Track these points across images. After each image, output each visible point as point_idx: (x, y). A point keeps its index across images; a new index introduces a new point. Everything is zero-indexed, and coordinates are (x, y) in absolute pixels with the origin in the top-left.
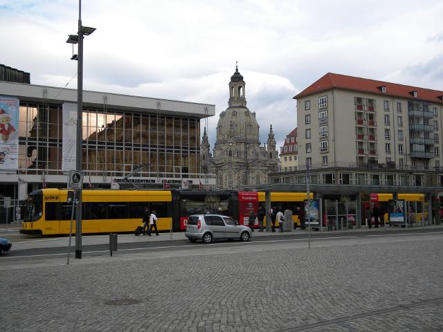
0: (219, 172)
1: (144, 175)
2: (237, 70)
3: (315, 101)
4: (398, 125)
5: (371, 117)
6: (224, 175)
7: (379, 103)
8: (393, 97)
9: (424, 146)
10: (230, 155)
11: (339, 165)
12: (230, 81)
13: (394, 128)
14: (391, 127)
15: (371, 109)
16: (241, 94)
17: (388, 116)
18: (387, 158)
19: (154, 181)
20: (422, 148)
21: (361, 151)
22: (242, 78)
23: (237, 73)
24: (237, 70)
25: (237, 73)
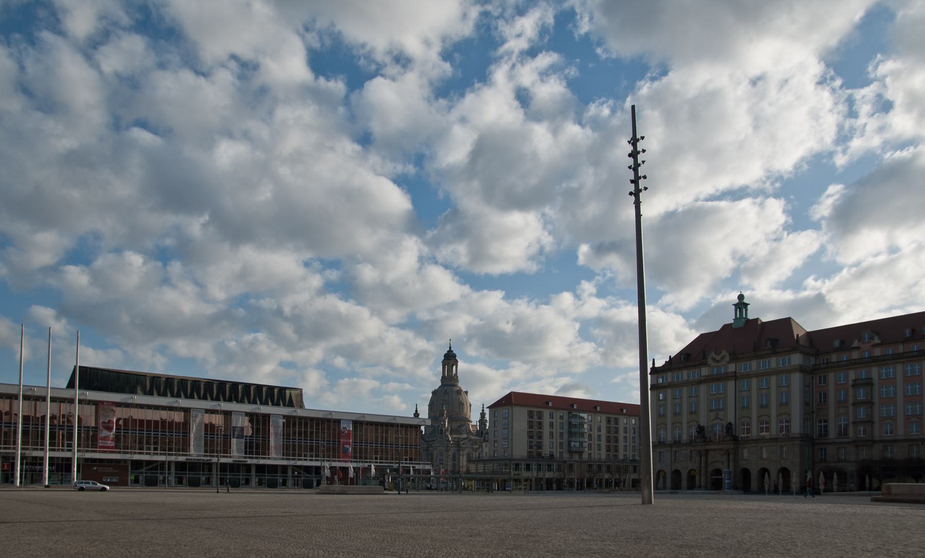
0: (430, 449)
1: (386, 463)
2: (450, 348)
3: (504, 411)
4: (560, 428)
5: (540, 423)
6: (435, 452)
7: (546, 413)
8: (557, 409)
9: (578, 443)
10: (442, 433)
11: (514, 457)
12: (443, 359)
13: (557, 430)
14: (554, 430)
15: (540, 418)
16: (454, 372)
17: (550, 420)
18: (550, 452)
19: (392, 466)
20: (577, 444)
21: (531, 447)
22: (455, 356)
23: (450, 351)
24: (450, 348)
25: (450, 351)
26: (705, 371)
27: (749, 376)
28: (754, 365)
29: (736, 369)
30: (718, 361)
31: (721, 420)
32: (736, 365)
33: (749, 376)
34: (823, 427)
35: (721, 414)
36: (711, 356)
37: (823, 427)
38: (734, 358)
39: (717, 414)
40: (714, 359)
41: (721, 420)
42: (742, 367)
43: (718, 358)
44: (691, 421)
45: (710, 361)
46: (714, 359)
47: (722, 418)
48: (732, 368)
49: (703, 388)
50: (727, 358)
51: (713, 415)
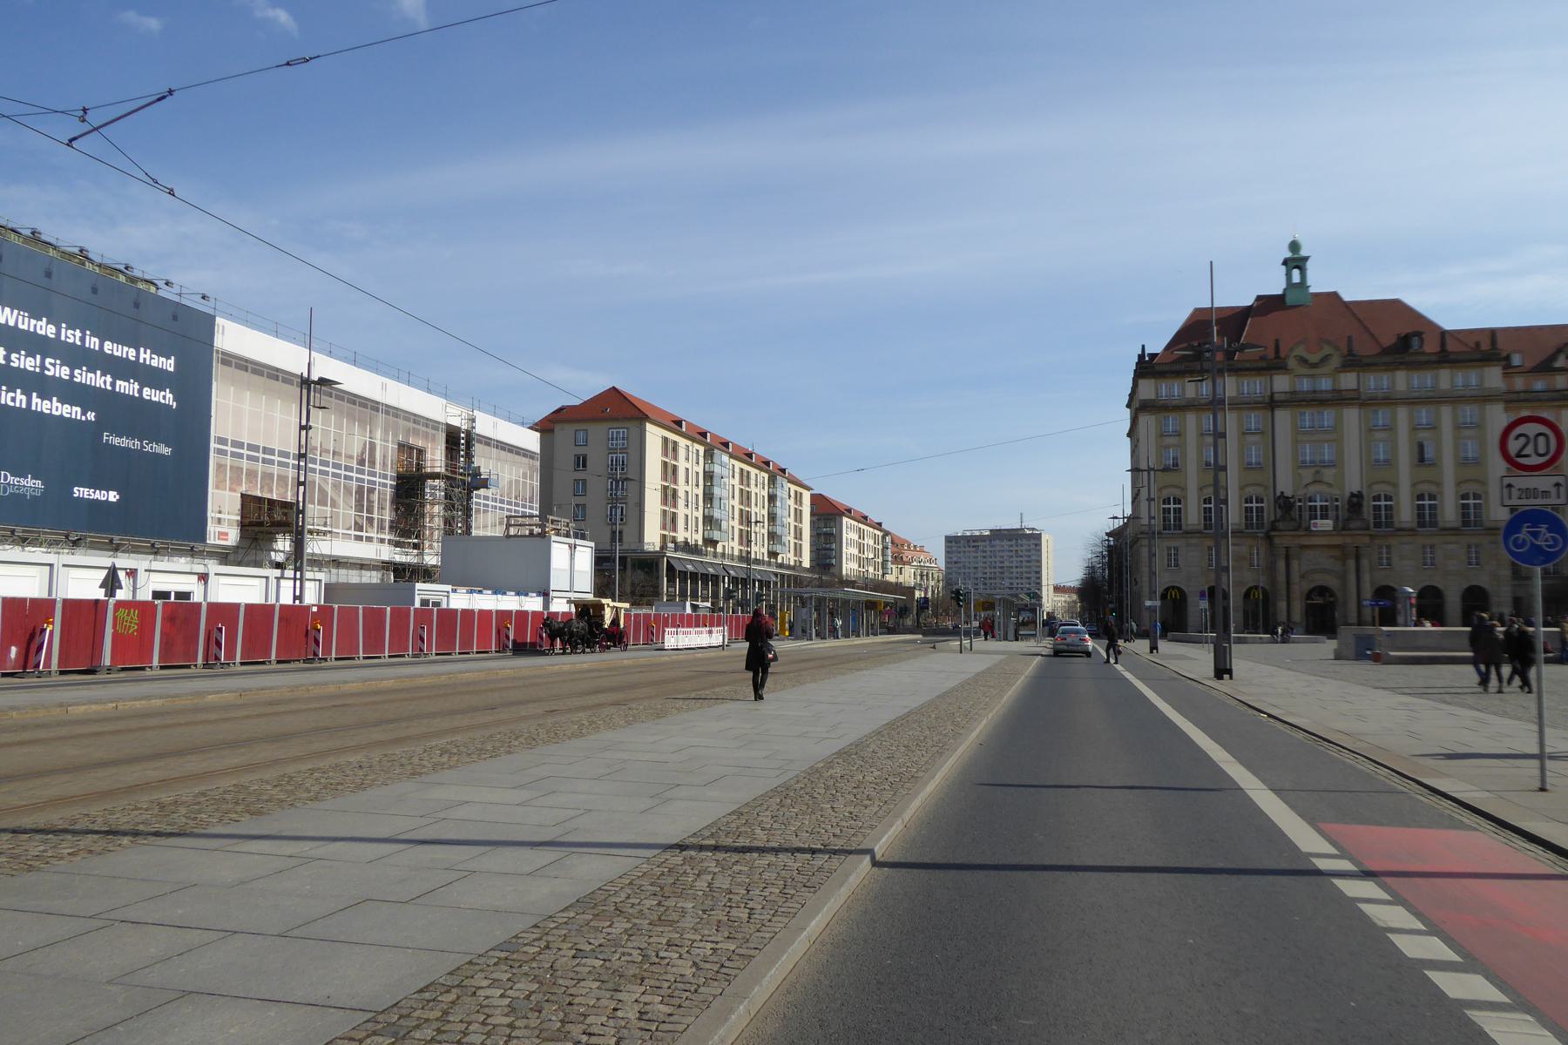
26: (1281, 383)
27: (1389, 401)
28: (1402, 381)
29: (1359, 384)
30: (1314, 366)
31: (1330, 485)
32: (1358, 375)
33: (1389, 401)
34: (1319, 510)
35: (1328, 474)
36: (1294, 353)
37: (1319, 510)
38: (1352, 362)
39: (1318, 472)
40: (1303, 361)
41: (1330, 485)
42: (1375, 382)
43: (1314, 358)
44: (1247, 485)
45: (1292, 363)
46: (1303, 361)
47: (1331, 482)
48: (1348, 381)
49: (1283, 417)
50: (1335, 362)
51: (1308, 475)
